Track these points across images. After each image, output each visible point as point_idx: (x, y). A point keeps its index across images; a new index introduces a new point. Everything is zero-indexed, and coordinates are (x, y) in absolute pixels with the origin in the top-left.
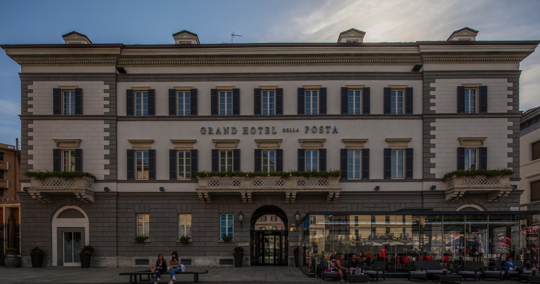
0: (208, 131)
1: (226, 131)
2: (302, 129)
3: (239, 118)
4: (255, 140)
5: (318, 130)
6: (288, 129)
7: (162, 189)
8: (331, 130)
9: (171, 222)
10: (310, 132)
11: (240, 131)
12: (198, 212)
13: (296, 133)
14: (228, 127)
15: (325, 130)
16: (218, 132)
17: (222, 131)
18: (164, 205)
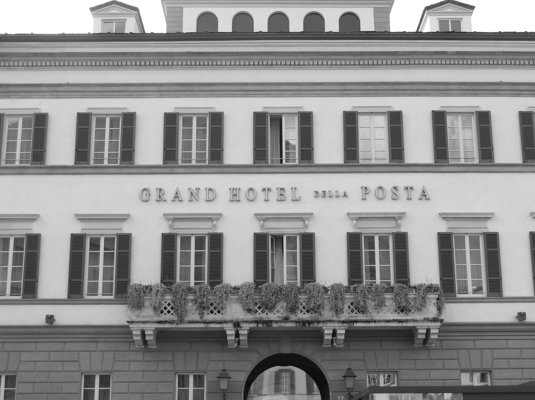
0: (154, 195)
1: (194, 196)
2: (355, 193)
3: (221, 170)
4: (256, 215)
5: (389, 194)
6: (324, 192)
7: (50, 319)
8: (416, 194)
9: (65, 391)
10: (371, 197)
11: (224, 195)
12: (126, 369)
13: (342, 200)
14: (198, 187)
15: (403, 194)
16: (177, 197)
17: (185, 195)
18: (52, 354)
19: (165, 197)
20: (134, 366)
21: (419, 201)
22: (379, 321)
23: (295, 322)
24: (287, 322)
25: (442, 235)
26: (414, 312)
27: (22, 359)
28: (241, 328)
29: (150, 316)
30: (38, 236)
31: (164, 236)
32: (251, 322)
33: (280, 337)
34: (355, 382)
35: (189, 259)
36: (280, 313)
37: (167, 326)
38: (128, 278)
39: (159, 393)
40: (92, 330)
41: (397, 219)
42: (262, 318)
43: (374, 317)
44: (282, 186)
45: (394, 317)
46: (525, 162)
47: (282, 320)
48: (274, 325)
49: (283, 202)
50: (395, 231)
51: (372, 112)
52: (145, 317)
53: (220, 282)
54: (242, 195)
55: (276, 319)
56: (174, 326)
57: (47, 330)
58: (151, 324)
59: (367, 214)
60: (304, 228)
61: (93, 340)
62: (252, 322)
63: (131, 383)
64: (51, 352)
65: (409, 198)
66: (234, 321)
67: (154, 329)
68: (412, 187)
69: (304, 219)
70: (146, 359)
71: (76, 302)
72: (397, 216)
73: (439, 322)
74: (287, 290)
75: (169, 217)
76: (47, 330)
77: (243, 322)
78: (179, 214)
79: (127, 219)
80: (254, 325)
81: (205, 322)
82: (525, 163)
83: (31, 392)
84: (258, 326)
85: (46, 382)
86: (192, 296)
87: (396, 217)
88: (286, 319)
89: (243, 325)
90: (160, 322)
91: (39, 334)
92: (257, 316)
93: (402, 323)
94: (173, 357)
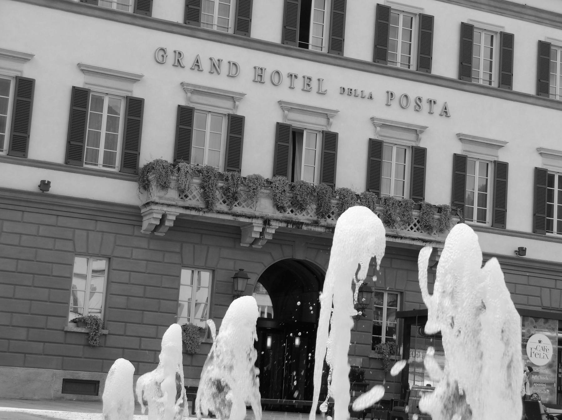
0: (171, 58)
1: (215, 67)
2: (380, 97)
3: (246, 43)
4: (280, 102)
5: (412, 104)
6: (351, 90)
7: (45, 185)
8: (438, 109)
9: (54, 274)
10: (395, 104)
11: (247, 73)
12: (128, 256)
13: (366, 101)
14: (220, 58)
15: (425, 106)
16: (197, 64)
17: (206, 65)
18: (42, 228)
19: (183, 63)
20: (137, 254)
21: (440, 117)
22: (406, 238)
23: (326, 227)
24: (317, 226)
25: (539, 170)
26: (436, 233)
27: (5, 230)
28: (270, 226)
29: (174, 200)
30: (87, 92)
31: (372, 141)
32: (281, 221)
33: (294, 241)
34: (247, 285)
35: (100, 122)
36: (309, 215)
37: (193, 213)
38: (27, 133)
39: (163, 287)
40: (92, 205)
41: (328, 117)
42: (291, 219)
43: (400, 233)
44: (309, 75)
45: (418, 235)
46: (539, 95)
47: (312, 223)
48: (304, 228)
49: (308, 93)
50: (414, 144)
51: (403, 11)
52: (168, 199)
53: (422, 200)
54: (267, 77)
55: (305, 221)
56: (201, 214)
57: (39, 198)
58: (176, 208)
59: (392, 122)
60: (327, 126)
61: (92, 217)
62: (283, 221)
63: (132, 273)
64: (40, 226)
65: (292, 87)
66: (265, 217)
67: (178, 214)
68: (436, 101)
69: (234, 100)
70: (151, 247)
71: (74, 170)
72: (419, 129)
73: (400, 238)
74: (321, 191)
75: (188, 87)
76: (39, 198)
77: (274, 220)
78: (200, 87)
79: (29, 60)
80: (283, 225)
81: (235, 215)
82: (538, 95)
83: (14, 270)
84: (287, 226)
85: (33, 261)
86: (222, 183)
87: (328, 115)
88: (316, 223)
89: (273, 223)
90: (187, 208)
91: (27, 201)
92: (286, 214)
93: (426, 243)
94: (181, 249)
